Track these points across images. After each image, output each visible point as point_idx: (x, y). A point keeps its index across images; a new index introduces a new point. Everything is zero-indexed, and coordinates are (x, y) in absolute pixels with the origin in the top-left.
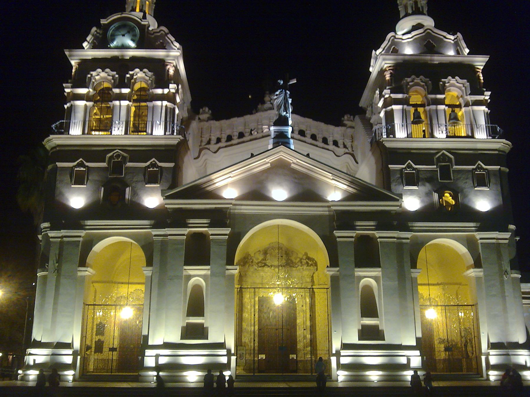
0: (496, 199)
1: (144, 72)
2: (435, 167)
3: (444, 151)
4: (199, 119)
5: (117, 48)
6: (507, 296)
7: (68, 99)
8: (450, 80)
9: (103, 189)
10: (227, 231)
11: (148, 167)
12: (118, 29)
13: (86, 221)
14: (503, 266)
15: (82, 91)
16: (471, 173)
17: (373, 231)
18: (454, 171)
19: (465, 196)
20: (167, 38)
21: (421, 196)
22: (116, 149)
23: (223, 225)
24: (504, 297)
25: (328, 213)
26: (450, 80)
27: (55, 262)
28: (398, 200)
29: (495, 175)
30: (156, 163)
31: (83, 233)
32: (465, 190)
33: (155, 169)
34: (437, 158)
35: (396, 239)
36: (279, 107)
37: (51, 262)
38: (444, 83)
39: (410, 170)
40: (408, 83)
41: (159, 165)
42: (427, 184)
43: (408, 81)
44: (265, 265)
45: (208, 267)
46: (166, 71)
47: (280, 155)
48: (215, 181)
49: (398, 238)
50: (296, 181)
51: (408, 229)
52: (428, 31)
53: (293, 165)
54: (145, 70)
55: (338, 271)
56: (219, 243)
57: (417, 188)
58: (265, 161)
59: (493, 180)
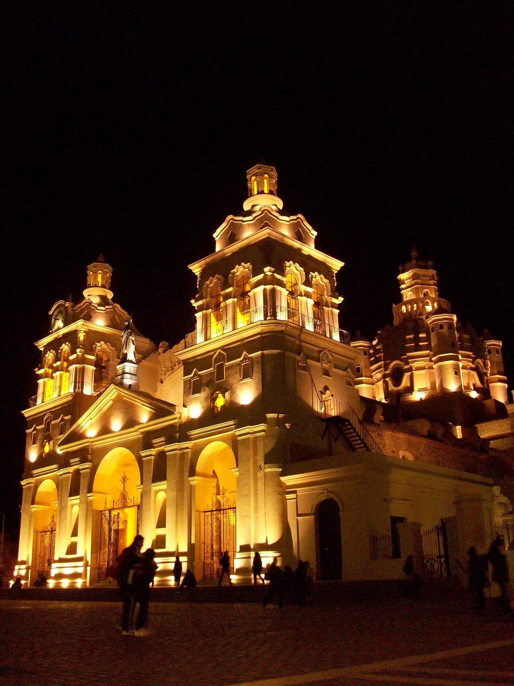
1: (67, 345)
2: (212, 369)
3: (219, 350)
5: (56, 331)
6: (260, 494)
10: (87, 465)
11: (60, 422)
15: (41, 371)
16: (239, 367)
19: (233, 393)
20: (91, 307)
22: (48, 413)
24: (256, 495)
26: (238, 269)
28: (173, 413)
29: (258, 362)
34: (215, 359)
39: (196, 378)
40: (208, 286)
42: (207, 389)
45: (78, 497)
48: (82, 425)
49: (180, 450)
51: (188, 439)
52: (231, 221)
55: (142, 488)
57: (200, 395)
59: (256, 369)
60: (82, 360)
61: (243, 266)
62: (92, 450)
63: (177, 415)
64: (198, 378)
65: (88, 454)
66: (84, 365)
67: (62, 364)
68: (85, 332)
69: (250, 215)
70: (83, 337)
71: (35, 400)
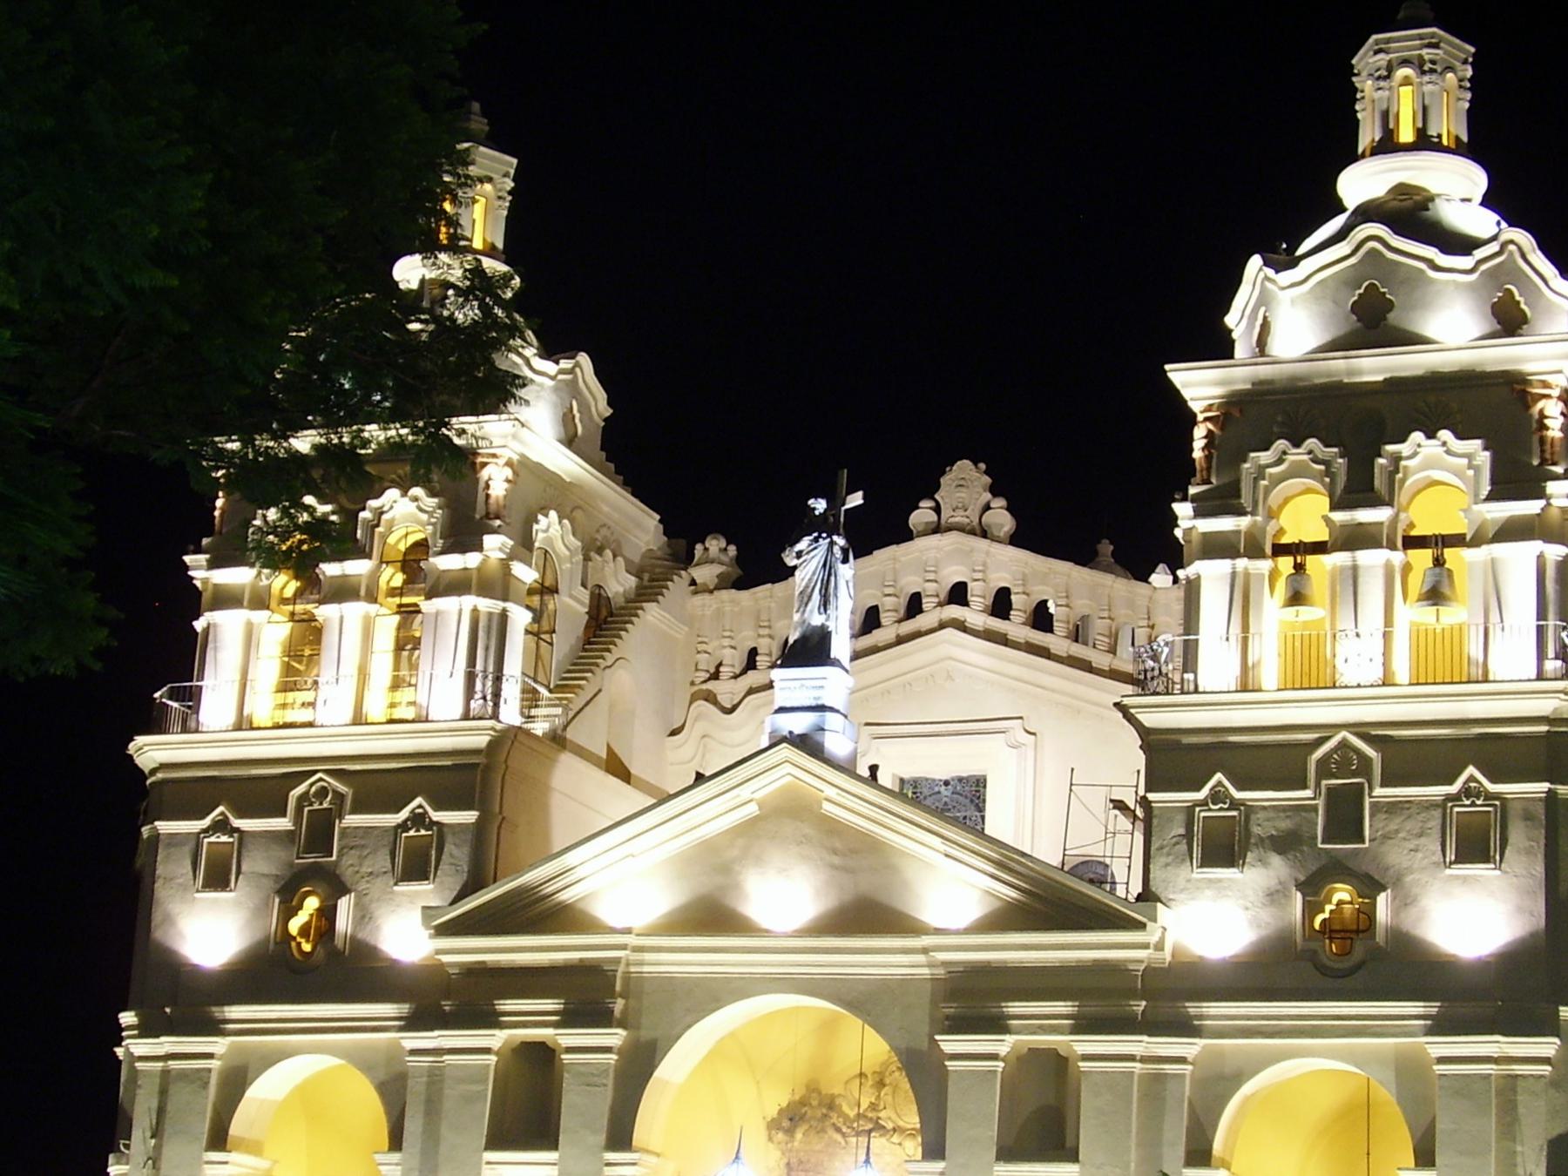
0: (1520, 910)
1: (416, 499)
2: (1308, 793)
3: (1344, 734)
4: (693, 582)
7: (206, 598)
8: (1419, 446)
9: (277, 900)
10: (614, 1037)
11: (404, 826)
13: (226, 1009)
14: (1519, 1159)
16: (1437, 813)
17: (1062, 1033)
18: (1376, 807)
19: (1404, 902)
21: (1250, 905)
22: (316, 772)
23: (598, 1017)
25: (926, 971)
26: (1419, 446)
27: (148, 1134)
28: (1141, 926)
29: (1528, 817)
30: (426, 812)
31: (219, 1045)
32: (1408, 879)
33: (423, 832)
34: (1323, 762)
35: (1138, 1065)
36: (806, 599)
37: (137, 1134)
38: (1397, 459)
40: (1260, 472)
41: (435, 819)
42: (1276, 860)
43: (1262, 462)
44: (878, 1127)
45: (552, 1156)
46: (482, 485)
47: (785, 772)
49: (1144, 1060)
50: (836, 860)
51: (1186, 1028)
53: (827, 806)
56: (590, 1077)
58: (738, 796)
59: (1517, 834)
60: (496, 584)
61: (1444, 444)
62: (627, 974)
63: (1151, 935)
64: (1234, 813)
65: (613, 995)
66: (510, 606)
67: (375, 576)
68: (509, 464)
69: (1469, 254)
70: (506, 485)
71: (191, 697)
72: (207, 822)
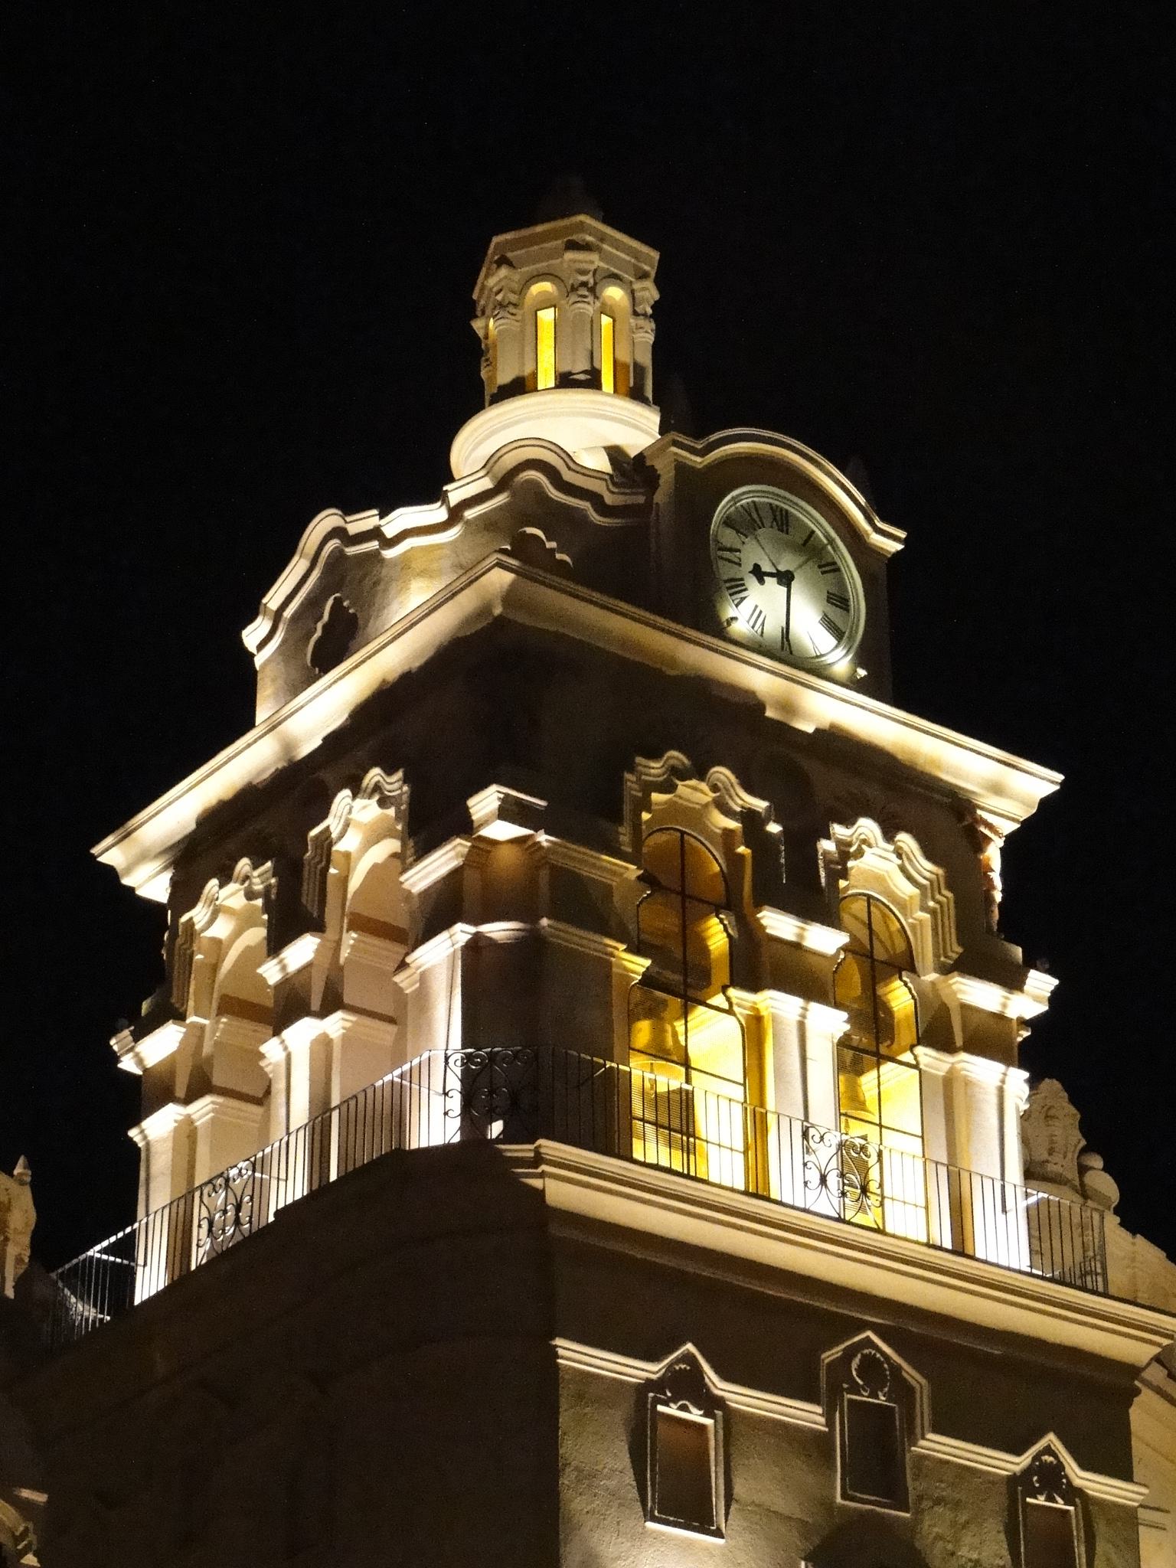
12: (746, 523)
22: (864, 1326)
30: (1060, 1466)
33: (1060, 1504)
54: (905, 839)
72: (653, 1370)
